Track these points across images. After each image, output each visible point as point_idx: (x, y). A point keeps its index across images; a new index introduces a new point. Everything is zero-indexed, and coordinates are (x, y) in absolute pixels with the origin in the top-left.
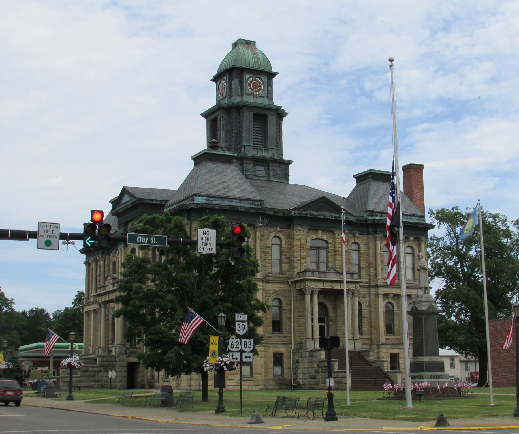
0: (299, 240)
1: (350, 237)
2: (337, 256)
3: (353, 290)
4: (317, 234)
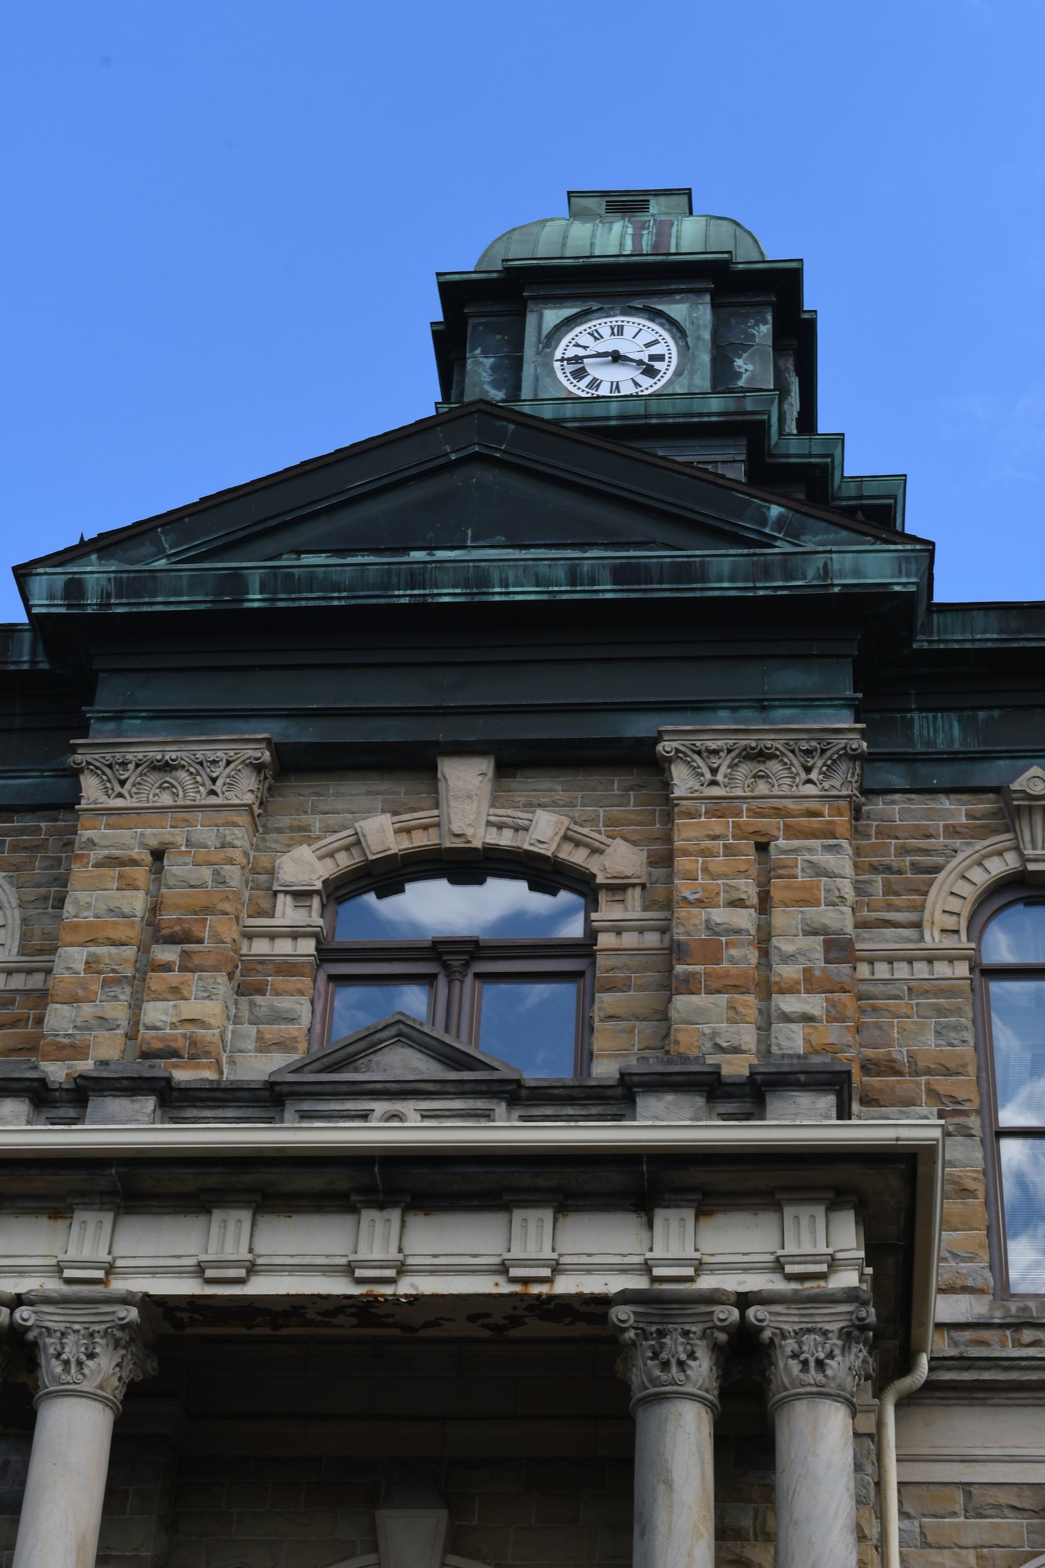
0: (140, 874)
1: (953, 831)
2: (682, 1003)
3: (744, 1300)
4: (437, 806)
